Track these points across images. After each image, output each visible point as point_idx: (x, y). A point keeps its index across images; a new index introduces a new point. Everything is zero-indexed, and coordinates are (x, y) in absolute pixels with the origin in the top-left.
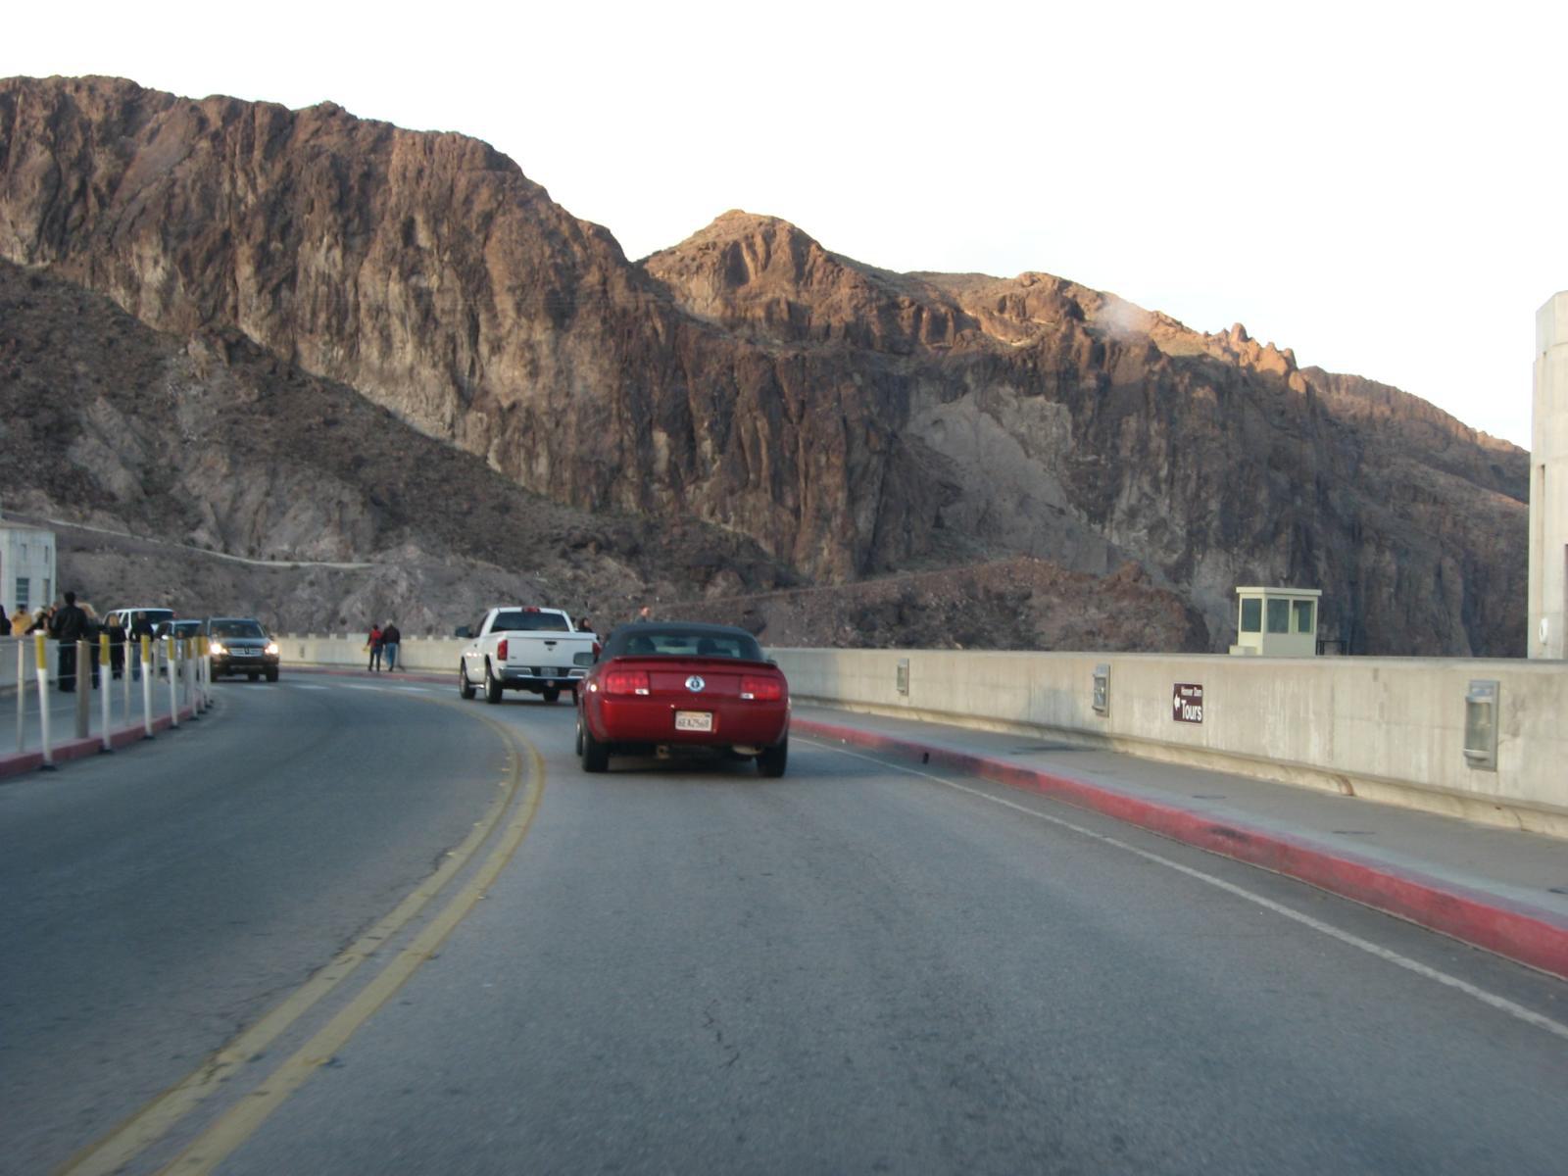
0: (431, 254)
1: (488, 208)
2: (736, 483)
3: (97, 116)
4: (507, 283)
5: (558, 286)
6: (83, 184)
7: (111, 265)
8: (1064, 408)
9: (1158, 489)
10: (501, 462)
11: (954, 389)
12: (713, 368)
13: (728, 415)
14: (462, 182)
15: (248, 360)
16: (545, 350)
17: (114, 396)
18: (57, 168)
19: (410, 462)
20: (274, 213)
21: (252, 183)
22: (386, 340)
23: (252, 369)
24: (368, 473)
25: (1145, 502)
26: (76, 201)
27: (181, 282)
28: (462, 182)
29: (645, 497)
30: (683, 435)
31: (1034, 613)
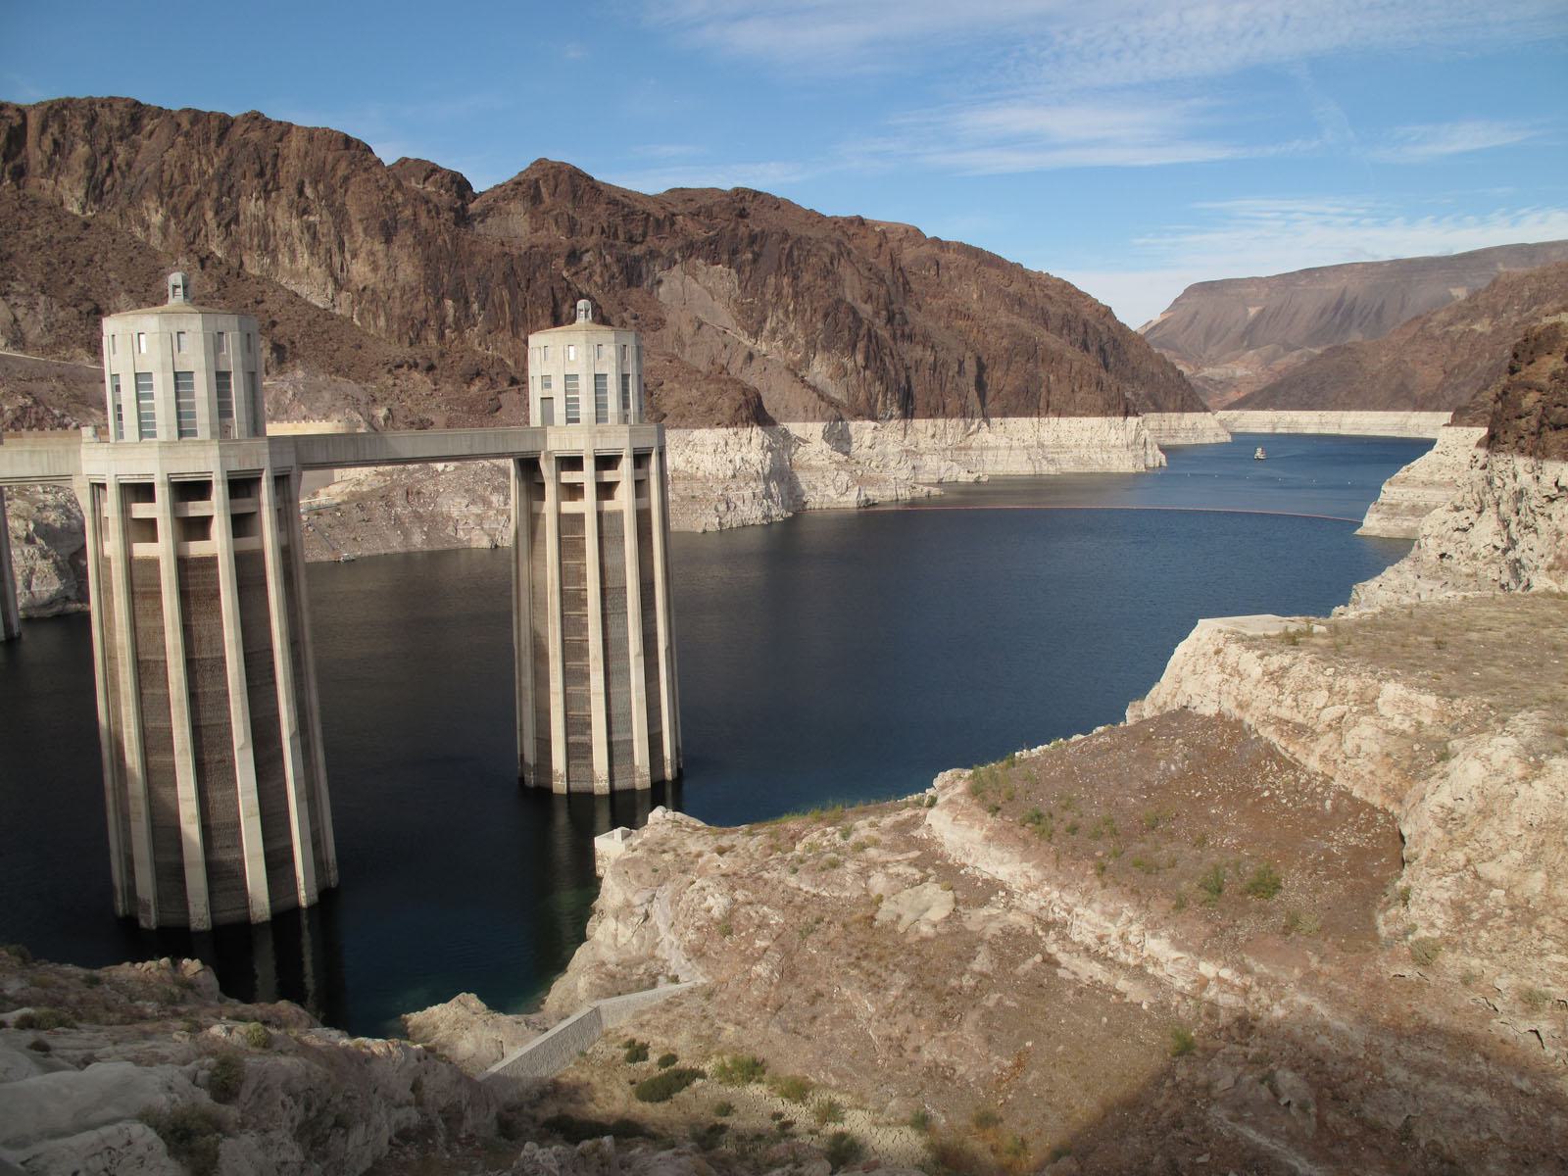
0: (314, 201)
1: (346, 173)
2: (492, 327)
3: (116, 123)
4: (358, 217)
5: (387, 218)
6: (111, 164)
7: (131, 212)
8: (733, 271)
9: (788, 317)
10: (359, 320)
11: (671, 263)
12: (479, 261)
13: (486, 288)
14: (330, 158)
15: (214, 267)
16: (381, 255)
17: (132, 292)
18: (94, 155)
19: (304, 323)
20: (223, 179)
21: (210, 161)
22: (293, 252)
23: (215, 272)
24: (278, 330)
25: (781, 325)
26: (107, 175)
27: (172, 222)
28: (330, 158)
29: (441, 336)
30: (462, 301)
31: (663, 394)
